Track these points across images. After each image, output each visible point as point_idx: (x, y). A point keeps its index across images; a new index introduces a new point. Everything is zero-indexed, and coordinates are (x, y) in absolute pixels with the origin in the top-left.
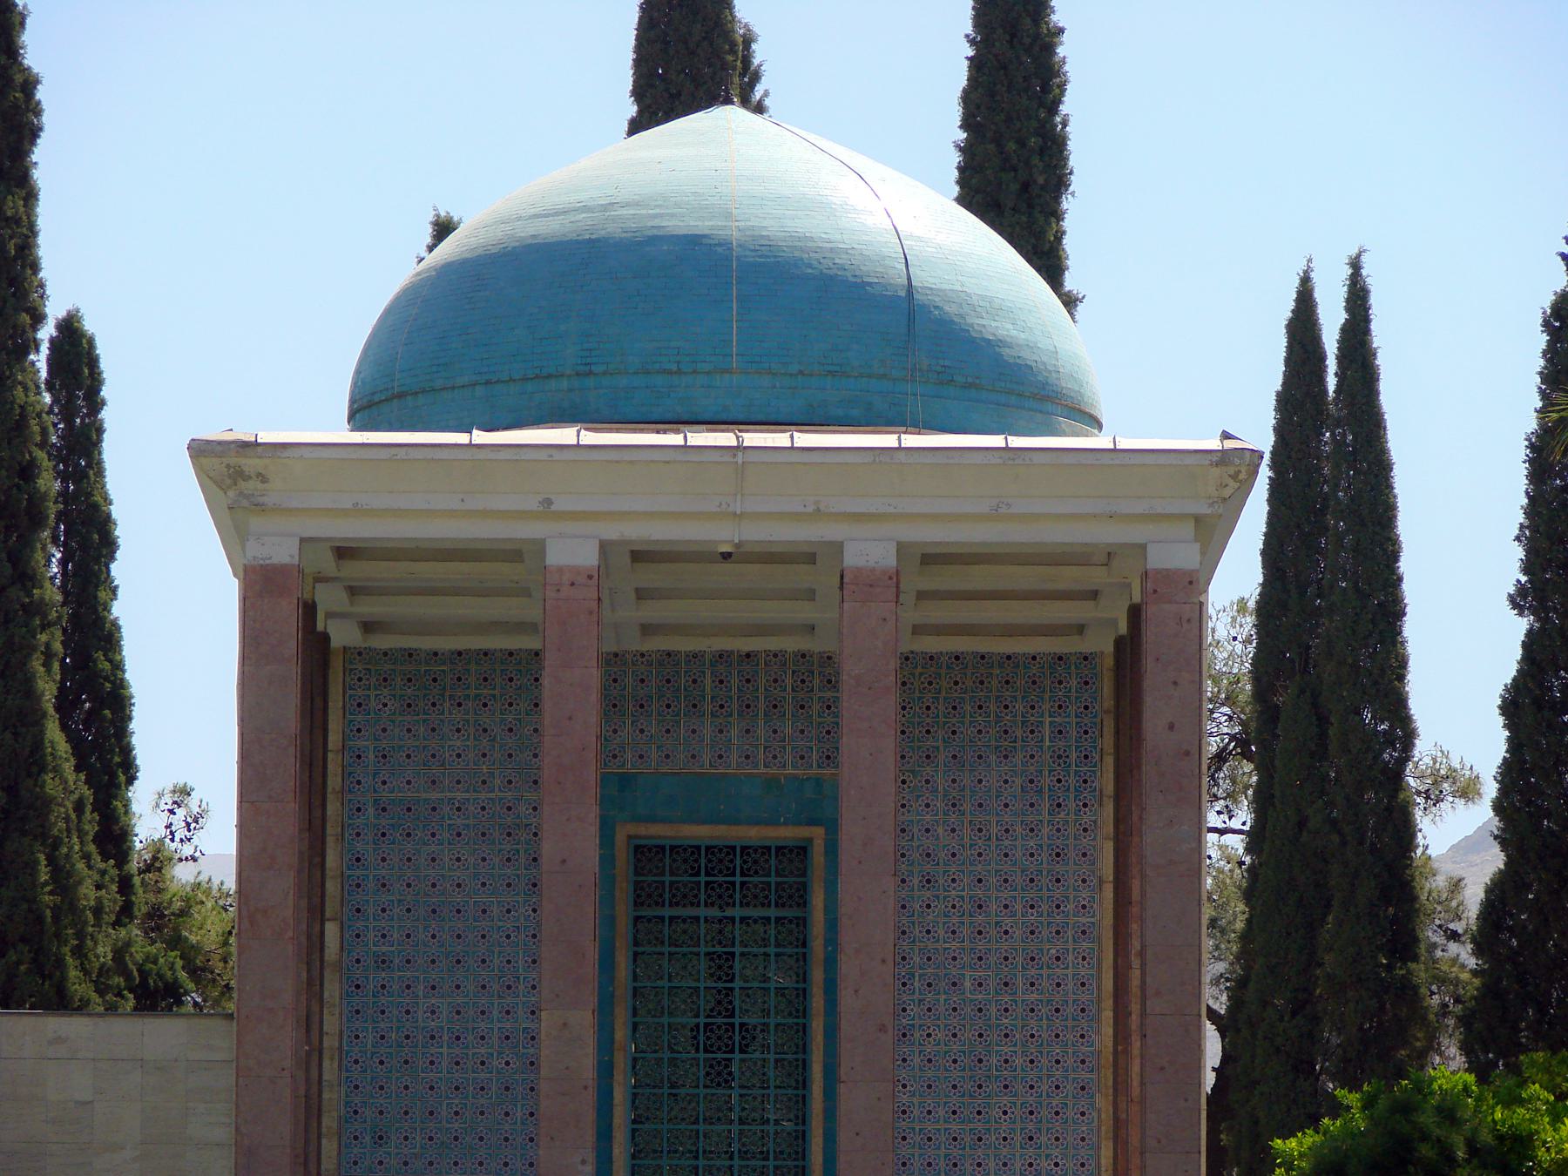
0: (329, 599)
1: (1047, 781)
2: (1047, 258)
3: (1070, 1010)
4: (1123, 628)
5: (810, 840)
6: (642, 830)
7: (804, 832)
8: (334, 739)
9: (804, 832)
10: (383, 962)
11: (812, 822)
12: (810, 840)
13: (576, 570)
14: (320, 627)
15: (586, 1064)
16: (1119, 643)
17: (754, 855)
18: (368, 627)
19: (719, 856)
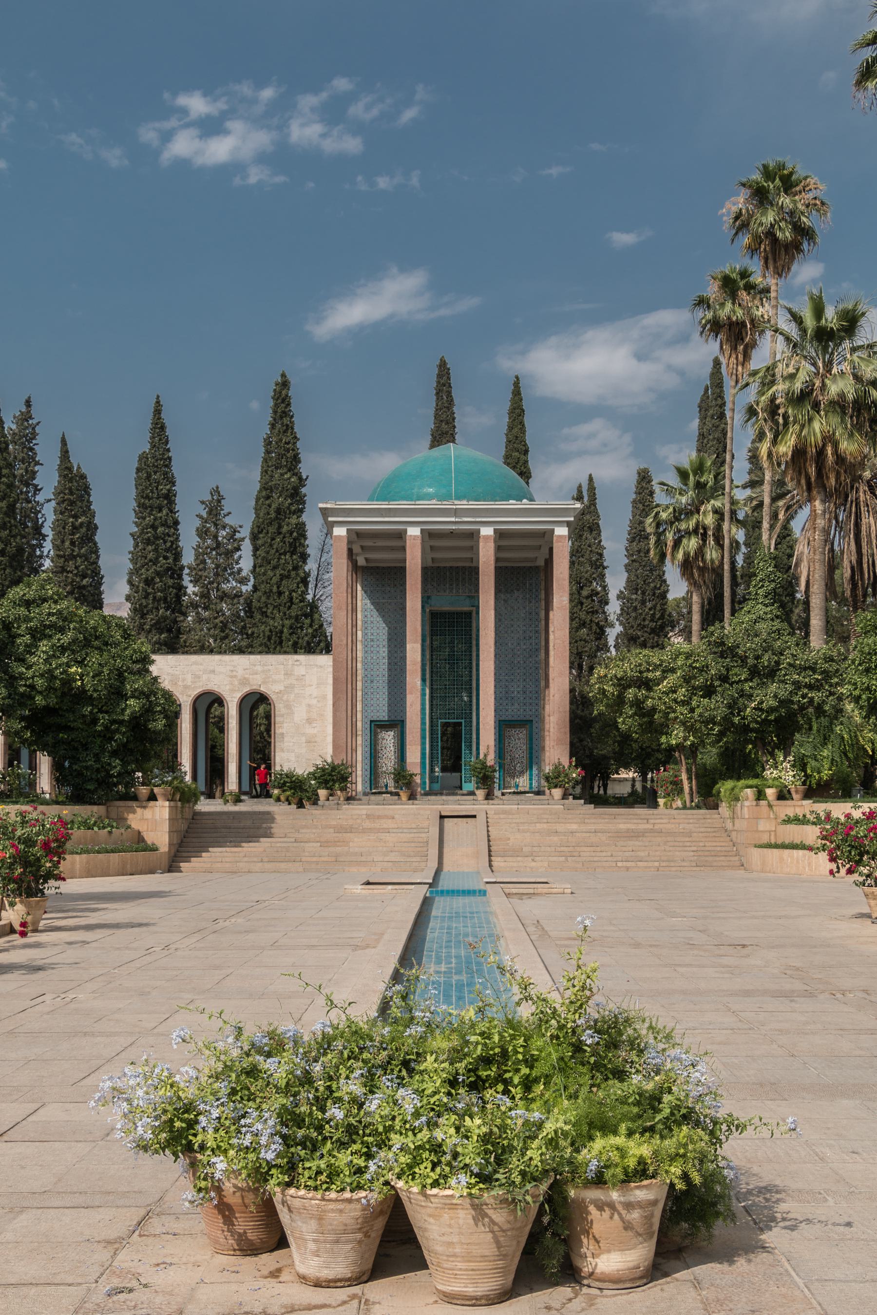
0: (356, 549)
1: (528, 596)
4: (548, 557)
7: (471, 608)
9: (471, 608)
10: (372, 640)
15: (419, 659)
17: (460, 614)
18: (367, 560)
19: (451, 614)
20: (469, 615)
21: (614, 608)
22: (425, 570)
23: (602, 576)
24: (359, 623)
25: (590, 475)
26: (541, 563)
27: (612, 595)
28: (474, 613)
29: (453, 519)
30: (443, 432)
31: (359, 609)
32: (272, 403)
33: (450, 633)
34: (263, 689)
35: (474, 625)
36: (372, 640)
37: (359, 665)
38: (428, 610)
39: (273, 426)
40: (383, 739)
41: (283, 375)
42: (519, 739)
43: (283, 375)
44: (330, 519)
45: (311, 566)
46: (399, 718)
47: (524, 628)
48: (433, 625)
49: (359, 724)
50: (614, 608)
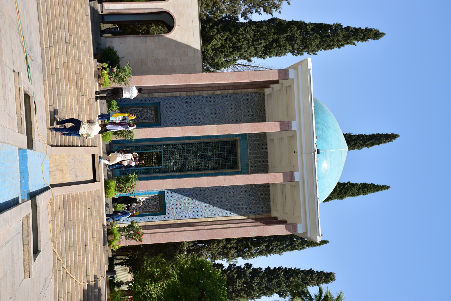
1: (250, 206)
2: (329, 199)
3: (214, 212)
5: (238, 169)
6: (238, 142)
7: (240, 168)
8: (250, 90)
9: (240, 168)
10: (215, 101)
11: (241, 169)
12: (238, 169)
13: (291, 126)
14: (272, 86)
16: (276, 218)
17: (236, 160)
18: (270, 95)
19: (235, 154)
20: (236, 167)
21: (241, 262)
22: (263, 136)
23: (261, 253)
24: (226, 92)
25: (328, 242)
26: (274, 214)
27: (250, 261)
28: (236, 170)
29: (304, 152)
30: (354, 141)
31: (236, 91)
32: (363, 27)
33: (224, 155)
34: (176, 28)
35: (229, 171)
36: (215, 101)
37: (197, 93)
38: (237, 138)
39: (348, 28)
40: (147, 112)
41: (383, 34)
42: (152, 206)
43: (383, 34)
44: (299, 67)
45: (256, 61)
46: (162, 122)
47: (229, 205)
48: (228, 142)
49: (156, 95)
50: (241, 262)
